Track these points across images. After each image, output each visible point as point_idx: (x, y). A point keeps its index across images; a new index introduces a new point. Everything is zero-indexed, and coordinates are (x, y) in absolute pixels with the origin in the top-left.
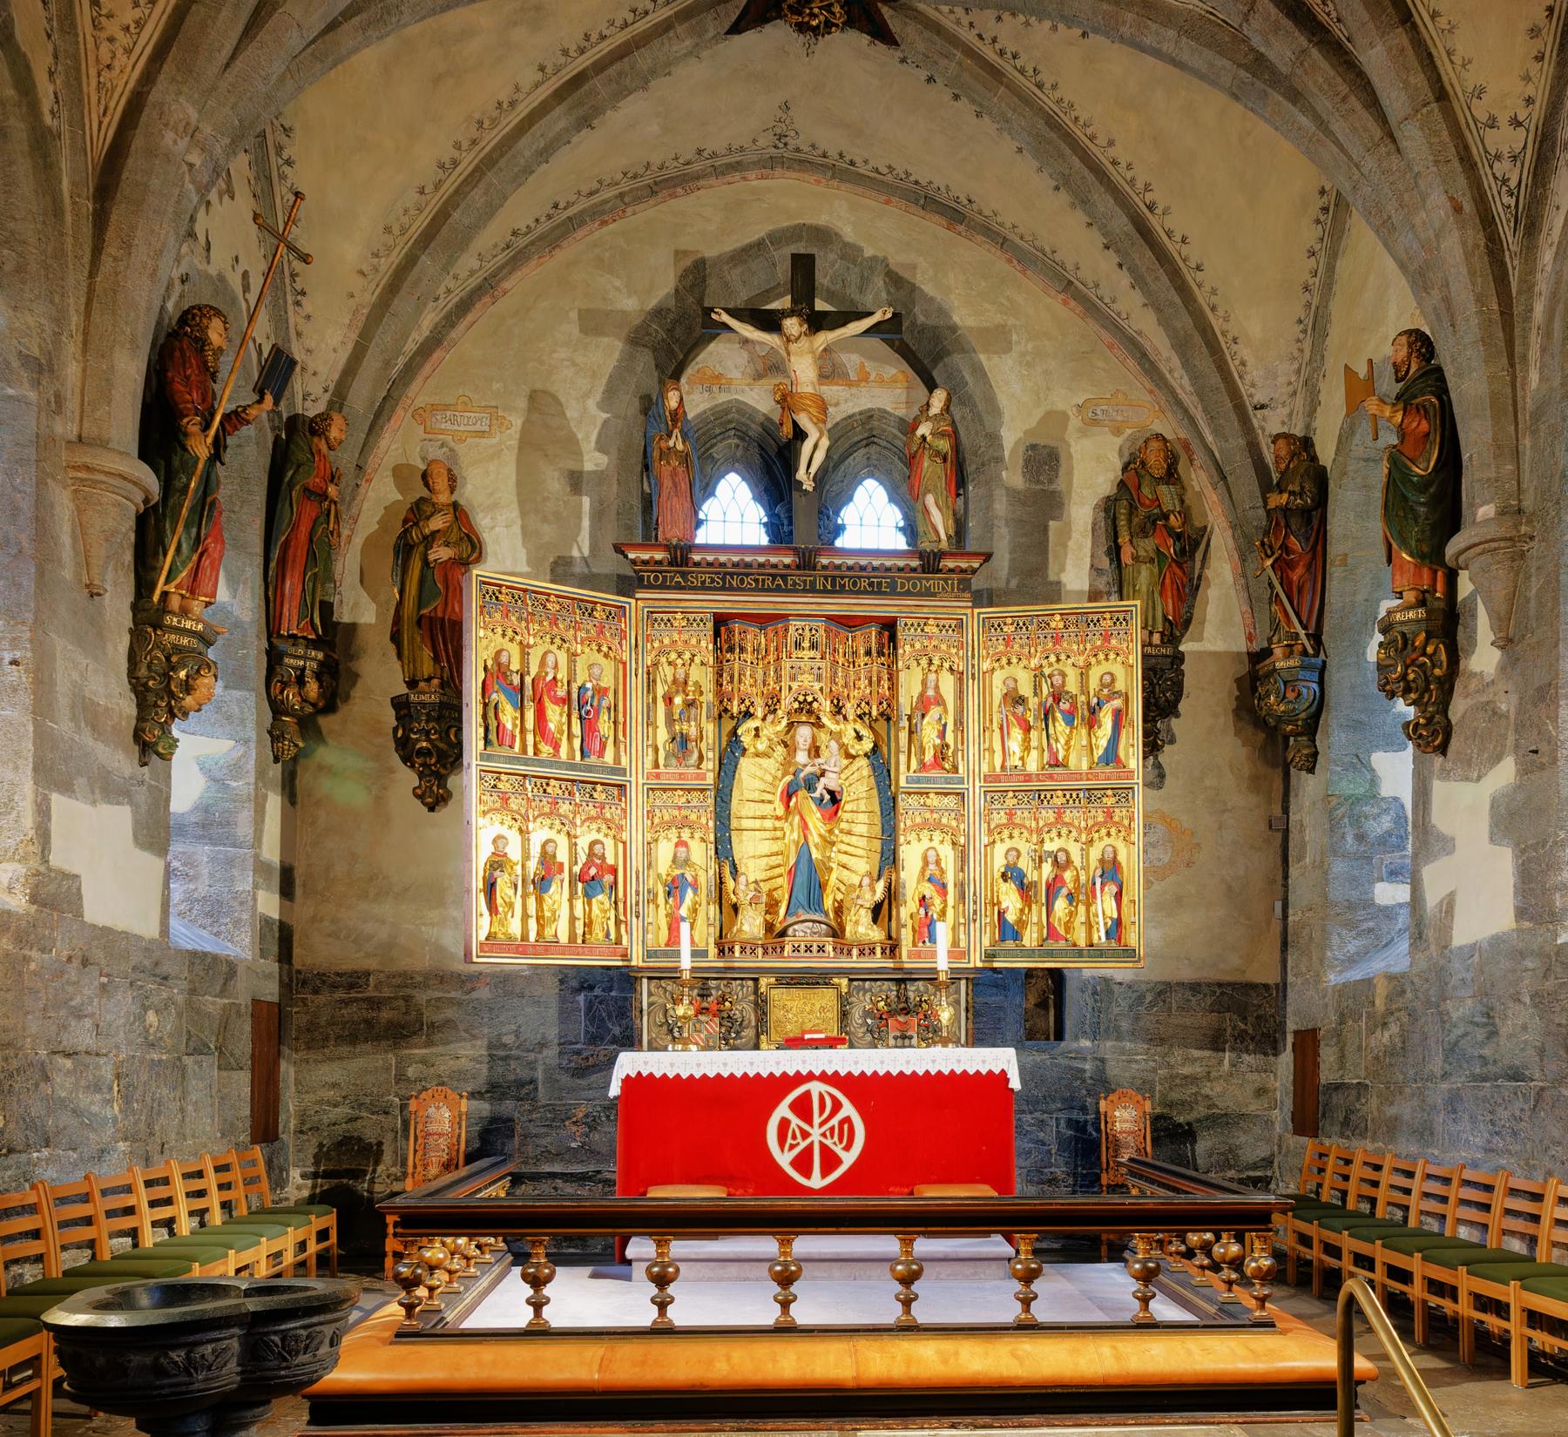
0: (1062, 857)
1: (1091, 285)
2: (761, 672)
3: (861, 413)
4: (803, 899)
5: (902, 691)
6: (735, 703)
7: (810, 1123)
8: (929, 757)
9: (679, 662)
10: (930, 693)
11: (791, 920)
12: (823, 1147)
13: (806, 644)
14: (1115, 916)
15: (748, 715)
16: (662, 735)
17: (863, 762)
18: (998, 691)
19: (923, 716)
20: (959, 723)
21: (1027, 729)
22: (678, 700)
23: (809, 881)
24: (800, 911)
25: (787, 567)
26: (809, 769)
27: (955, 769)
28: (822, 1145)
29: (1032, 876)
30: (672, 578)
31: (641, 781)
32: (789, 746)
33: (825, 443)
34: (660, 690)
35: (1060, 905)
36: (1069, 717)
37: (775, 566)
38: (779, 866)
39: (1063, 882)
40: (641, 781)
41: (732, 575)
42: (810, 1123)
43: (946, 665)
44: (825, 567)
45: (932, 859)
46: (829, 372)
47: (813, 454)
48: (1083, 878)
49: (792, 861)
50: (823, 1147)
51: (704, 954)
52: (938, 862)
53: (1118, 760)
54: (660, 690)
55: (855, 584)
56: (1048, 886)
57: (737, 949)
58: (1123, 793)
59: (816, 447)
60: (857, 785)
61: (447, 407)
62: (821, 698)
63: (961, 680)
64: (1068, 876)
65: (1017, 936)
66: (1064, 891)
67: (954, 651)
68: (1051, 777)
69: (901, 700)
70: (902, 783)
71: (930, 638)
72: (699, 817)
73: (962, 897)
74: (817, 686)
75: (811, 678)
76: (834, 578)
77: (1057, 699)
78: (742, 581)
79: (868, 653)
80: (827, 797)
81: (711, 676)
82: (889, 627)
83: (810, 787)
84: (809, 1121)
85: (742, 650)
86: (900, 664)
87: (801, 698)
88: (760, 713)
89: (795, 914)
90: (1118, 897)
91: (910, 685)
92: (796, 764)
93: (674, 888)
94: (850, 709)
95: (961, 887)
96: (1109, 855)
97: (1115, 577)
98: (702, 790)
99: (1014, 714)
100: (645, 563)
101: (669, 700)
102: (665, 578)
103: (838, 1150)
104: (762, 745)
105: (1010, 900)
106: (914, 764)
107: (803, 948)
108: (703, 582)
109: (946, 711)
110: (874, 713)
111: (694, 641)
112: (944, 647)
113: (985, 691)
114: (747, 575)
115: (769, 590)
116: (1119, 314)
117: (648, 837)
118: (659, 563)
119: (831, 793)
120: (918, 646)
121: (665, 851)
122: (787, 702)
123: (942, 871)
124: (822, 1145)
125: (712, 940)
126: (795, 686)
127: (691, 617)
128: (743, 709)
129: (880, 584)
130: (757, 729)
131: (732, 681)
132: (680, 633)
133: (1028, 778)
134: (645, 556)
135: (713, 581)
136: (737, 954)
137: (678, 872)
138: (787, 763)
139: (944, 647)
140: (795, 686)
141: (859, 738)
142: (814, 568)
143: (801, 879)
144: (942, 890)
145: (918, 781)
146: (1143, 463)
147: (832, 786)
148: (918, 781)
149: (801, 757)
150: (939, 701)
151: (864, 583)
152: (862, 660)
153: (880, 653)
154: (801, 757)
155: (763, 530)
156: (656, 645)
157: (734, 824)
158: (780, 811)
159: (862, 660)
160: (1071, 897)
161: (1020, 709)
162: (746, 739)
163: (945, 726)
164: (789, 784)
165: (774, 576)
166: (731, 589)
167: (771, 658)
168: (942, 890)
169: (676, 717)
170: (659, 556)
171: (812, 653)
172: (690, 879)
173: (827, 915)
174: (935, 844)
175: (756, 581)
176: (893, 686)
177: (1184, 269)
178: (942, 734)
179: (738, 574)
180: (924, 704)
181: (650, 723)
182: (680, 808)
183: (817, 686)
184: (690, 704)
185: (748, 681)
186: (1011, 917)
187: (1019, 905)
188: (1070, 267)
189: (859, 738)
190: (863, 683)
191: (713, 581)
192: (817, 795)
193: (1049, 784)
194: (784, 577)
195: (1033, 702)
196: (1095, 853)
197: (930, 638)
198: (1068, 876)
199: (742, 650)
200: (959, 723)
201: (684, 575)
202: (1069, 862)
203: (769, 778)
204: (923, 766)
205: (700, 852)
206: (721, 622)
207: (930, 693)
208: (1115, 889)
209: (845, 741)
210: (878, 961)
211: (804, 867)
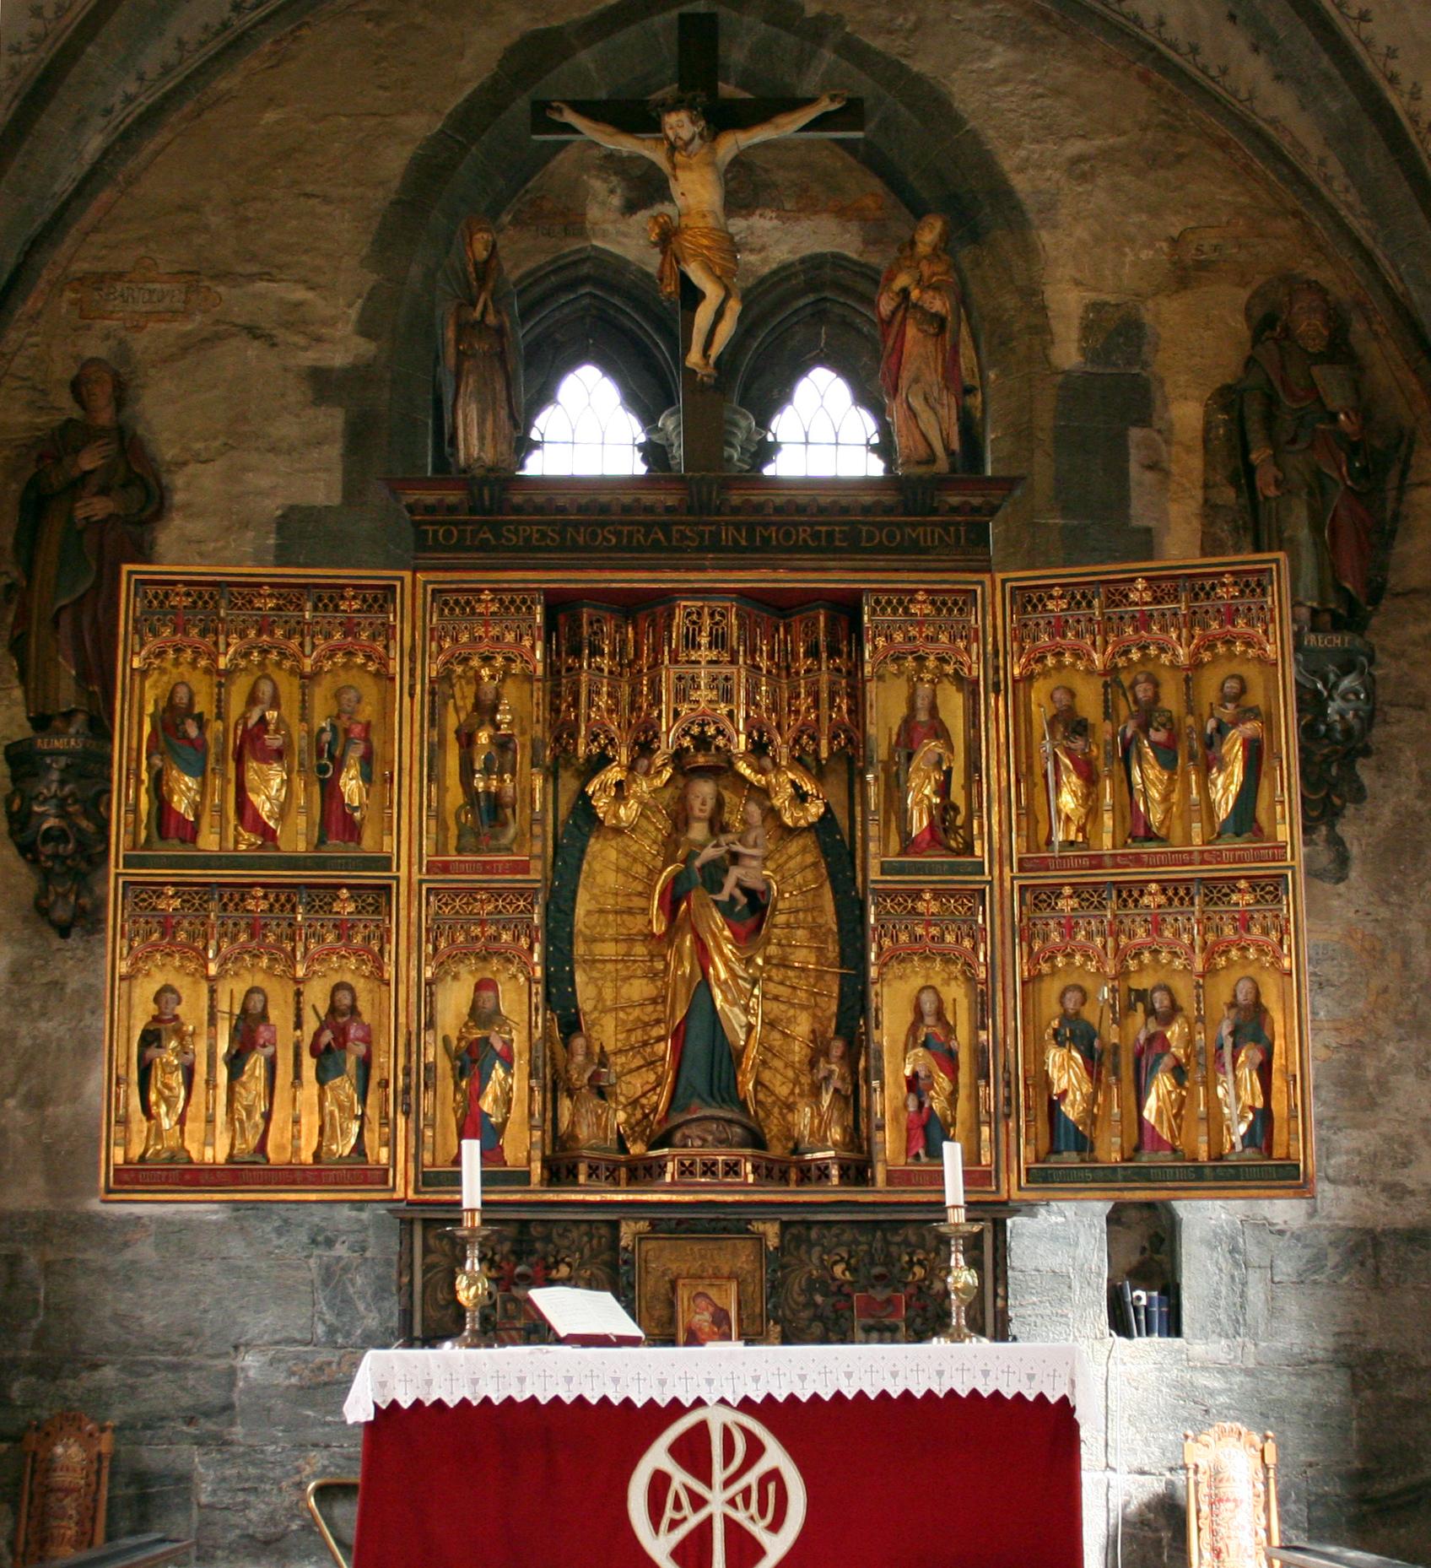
0: (1160, 1001)
1: (1184, 49)
2: (627, 689)
3: (803, 261)
4: (701, 1083)
5: (872, 715)
6: (581, 741)
7: (707, 1480)
8: (919, 823)
9: (485, 672)
10: (922, 717)
11: (678, 1119)
12: (731, 1525)
13: (704, 641)
14: (1259, 1104)
15: (601, 762)
16: (455, 796)
17: (808, 840)
18: (1040, 714)
19: (910, 757)
20: (973, 766)
21: (1090, 778)
22: (483, 737)
23: (706, 1062)
24: (696, 1102)
25: (669, 510)
26: (709, 853)
27: (969, 848)
28: (729, 1522)
29: (1112, 1035)
30: (474, 534)
31: (416, 877)
32: (680, 819)
33: (734, 307)
34: (452, 722)
35: (1161, 1086)
36: (1167, 756)
37: (649, 510)
38: (658, 1022)
39: (1166, 1045)
40: (416, 877)
41: (576, 525)
42: (707, 1480)
43: (949, 669)
44: (736, 510)
45: (928, 1005)
46: (744, 188)
47: (714, 323)
48: (1200, 1038)
49: (680, 1014)
50: (731, 1525)
51: (523, 1178)
52: (940, 1014)
53: (1258, 832)
54: (452, 722)
55: (788, 535)
56: (1139, 1055)
57: (583, 1168)
58: (1270, 887)
59: (719, 314)
60: (791, 877)
61: (120, 276)
62: (730, 730)
63: (975, 694)
64: (1174, 1032)
65: (1083, 1144)
66: (1167, 1061)
67: (961, 644)
68: (1138, 860)
69: (872, 730)
70: (874, 874)
71: (920, 624)
72: (516, 938)
73: (981, 1072)
74: (723, 709)
75: (713, 695)
76: (751, 528)
77: (1145, 727)
78: (594, 535)
79: (813, 652)
80: (744, 900)
81: (538, 695)
82: (845, 610)
83: (713, 875)
84: (706, 1478)
85: (596, 651)
86: (868, 669)
87: (696, 730)
88: (624, 757)
89: (685, 1109)
90: (1264, 1071)
91: (886, 708)
92: (691, 842)
93: (472, 1061)
94: (781, 747)
95: (980, 1054)
96: (1244, 994)
97: (1246, 517)
98: (521, 893)
99: (1069, 753)
100: (429, 509)
101: (467, 740)
102: (462, 533)
103: (758, 1530)
104: (628, 812)
105: (1065, 1072)
106: (895, 843)
107: (698, 1168)
108: (528, 539)
109: (950, 747)
110: (824, 754)
111: (510, 637)
112: (943, 638)
113: (1021, 715)
114: (602, 525)
115: (641, 549)
116: (1234, 94)
117: (428, 973)
118: (452, 509)
119: (748, 892)
120: (899, 637)
121: (454, 1001)
122: (669, 739)
123: (950, 1030)
124: (729, 1522)
125: (536, 1154)
126: (684, 709)
127: (507, 598)
128: (595, 749)
129: (830, 535)
130: (619, 785)
131: (576, 704)
132: (486, 624)
133: (1097, 862)
134: (429, 498)
135: (544, 535)
136: (582, 1179)
137: (477, 1034)
138: (670, 845)
139: (943, 638)
140: (684, 709)
141: (801, 797)
142: (719, 512)
143: (697, 1046)
144: (949, 1062)
145: (900, 869)
146: (1287, 330)
147: (752, 882)
148: (900, 869)
149: (698, 831)
150: (939, 731)
151: (803, 534)
152: (803, 664)
153: (833, 652)
154: (698, 831)
155: (639, 455)
156: (447, 644)
157: (580, 949)
158: (658, 927)
159: (803, 664)
160: (1179, 1073)
161: (1079, 744)
162: (601, 804)
163: (948, 774)
164: (675, 879)
165: (649, 526)
166: (575, 548)
167: (644, 663)
168: (949, 1062)
169: (478, 765)
170: (453, 497)
171: (713, 655)
172: (498, 1046)
173: (743, 1105)
174: (936, 982)
175: (618, 534)
176: (858, 708)
177: (1340, 22)
178: (944, 789)
179: (588, 524)
180: (907, 740)
181: (435, 774)
182: (482, 923)
183: (723, 709)
184: (503, 744)
185: (603, 701)
186: (1071, 1110)
187: (1087, 1088)
188: (1149, 22)
189: (801, 797)
190: (804, 703)
191: (544, 535)
192: (724, 896)
193: (1132, 874)
194: (666, 527)
195: (1104, 730)
196: (1221, 991)
197: (920, 624)
198: (1174, 1032)
199: (596, 651)
200: (973, 766)
201: (495, 528)
202: (1174, 1010)
203: (639, 870)
204: (908, 844)
205: (516, 1000)
206: (560, 606)
207: (922, 717)
208: (1258, 1057)
209: (777, 802)
210: (833, 1189)
211: (699, 1027)
